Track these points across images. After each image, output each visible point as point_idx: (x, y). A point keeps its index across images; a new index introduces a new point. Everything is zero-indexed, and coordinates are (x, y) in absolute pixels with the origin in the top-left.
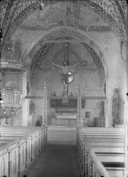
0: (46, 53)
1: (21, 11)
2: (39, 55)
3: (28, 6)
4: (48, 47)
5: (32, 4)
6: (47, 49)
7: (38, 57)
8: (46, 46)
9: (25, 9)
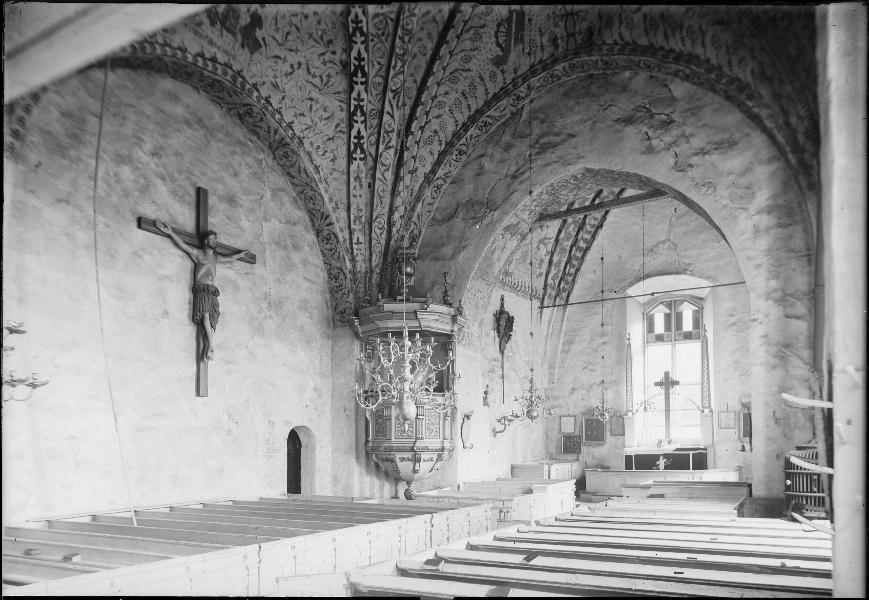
1: (443, 142)
2: (565, 259)
3: (460, 123)
4: (592, 226)
5: (472, 113)
9: (454, 135)
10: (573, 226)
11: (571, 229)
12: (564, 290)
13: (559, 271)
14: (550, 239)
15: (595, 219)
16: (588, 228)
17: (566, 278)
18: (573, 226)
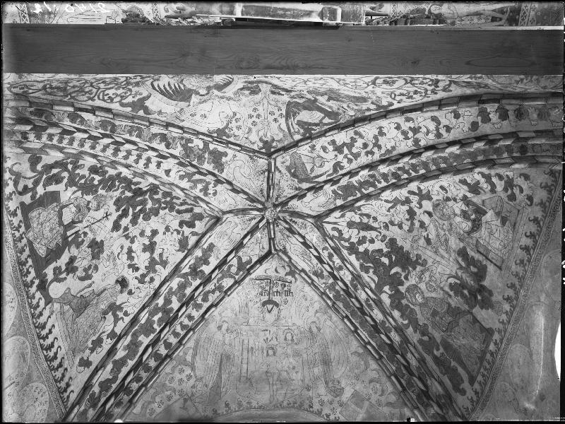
0: (167, 356)
2: (131, 363)
4: (183, 327)
6: (176, 334)
7: (125, 370)
8: (176, 317)
10: (160, 315)
11: (156, 318)
13: (115, 379)
14: (126, 314)
15: (190, 318)
17: (121, 395)
18: (160, 315)
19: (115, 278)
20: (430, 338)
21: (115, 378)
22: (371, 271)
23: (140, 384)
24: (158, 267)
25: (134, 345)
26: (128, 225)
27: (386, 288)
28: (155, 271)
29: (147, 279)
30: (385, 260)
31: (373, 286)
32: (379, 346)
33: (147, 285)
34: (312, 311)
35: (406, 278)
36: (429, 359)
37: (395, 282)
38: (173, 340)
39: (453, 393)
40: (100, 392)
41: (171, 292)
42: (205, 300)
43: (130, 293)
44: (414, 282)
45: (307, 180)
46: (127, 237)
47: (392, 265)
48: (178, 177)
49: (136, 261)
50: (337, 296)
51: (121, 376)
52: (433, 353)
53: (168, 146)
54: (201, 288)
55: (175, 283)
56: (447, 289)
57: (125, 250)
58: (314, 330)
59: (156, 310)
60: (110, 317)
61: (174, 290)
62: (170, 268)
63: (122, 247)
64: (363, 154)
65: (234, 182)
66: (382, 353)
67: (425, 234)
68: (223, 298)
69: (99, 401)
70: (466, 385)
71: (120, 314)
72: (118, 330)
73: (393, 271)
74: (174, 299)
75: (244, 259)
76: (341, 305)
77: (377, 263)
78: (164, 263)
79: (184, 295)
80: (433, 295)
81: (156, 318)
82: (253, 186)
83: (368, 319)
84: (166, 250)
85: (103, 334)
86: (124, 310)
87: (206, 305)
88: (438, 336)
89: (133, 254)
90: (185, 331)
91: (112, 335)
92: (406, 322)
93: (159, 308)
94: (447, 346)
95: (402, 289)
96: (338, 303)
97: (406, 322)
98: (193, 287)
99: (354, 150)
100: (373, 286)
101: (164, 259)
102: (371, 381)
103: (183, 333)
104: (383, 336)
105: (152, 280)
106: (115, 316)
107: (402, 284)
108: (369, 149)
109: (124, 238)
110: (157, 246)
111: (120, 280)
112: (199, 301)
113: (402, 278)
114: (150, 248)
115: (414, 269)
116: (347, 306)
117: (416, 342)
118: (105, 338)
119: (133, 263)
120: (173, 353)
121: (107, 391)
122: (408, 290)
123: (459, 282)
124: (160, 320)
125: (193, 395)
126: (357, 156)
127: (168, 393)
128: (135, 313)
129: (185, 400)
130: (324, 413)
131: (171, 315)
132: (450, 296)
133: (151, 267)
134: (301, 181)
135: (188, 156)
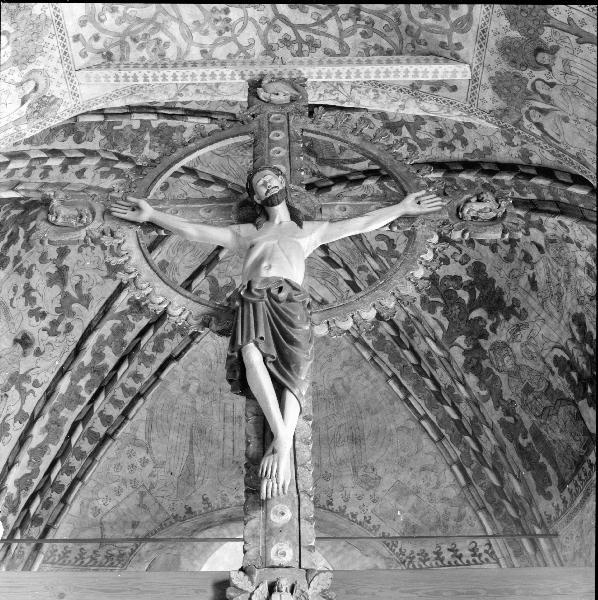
2: (54, 450)
4: (127, 392)
8: (113, 379)
10: (88, 377)
11: (82, 383)
12: (37, 520)
13: (36, 471)
14: (36, 384)
15: (136, 377)
16: (119, 394)
18: (88, 377)
19: (13, 338)
20: (516, 420)
21: (36, 471)
22: (439, 309)
23: (74, 476)
24: (75, 306)
25: (56, 423)
26: (19, 252)
27: (461, 340)
28: (72, 314)
29: (61, 328)
30: (464, 296)
31: (440, 333)
32: (440, 422)
33: (61, 338)
34: (337, 363)
35: (493, 329)
36: (510, 447)
37: (476, 333)
38: (115, 413)
39: (536, 495)
40: (19, 492)
41: (101, 342)
42: (158, 348)
43: (38, 353)
44: (503, 339)
45: (333, 162)
46: (19, 271)
47: (473, 306)
48: (98, 176)
49: (39, 303)
50: (381, 341)
51: (44, 467)
52: (517, 439)
53: (78, 140)
54: (151, 332)
55: (106, 329)
56: (550, 361)
57: (21, 291)
58: (340, 389)
59: (83, 371)
60: (14, 393)
61: (105, 338)
62: (96, 307)
63: (15, 290)
64: (435, 145)
65: (198, 168)
66: (443, 431)
67: (530, 272)
68: (189, 346)
69: (19, 502)
70: (553, 489)
71: (28, 386)
72: (29, 408)
73: (475, 314)
74: (108, 351)
75: (222, 282)
76: (385, 357)
77: (449, 298)
78: (86, 300)
79: (123, 343)
80: (530, 364)
81: (82, 383)
82: (235, 167)
83: (428, 382)
84: (85, 279)
85: (8, 418)
86: (32, 380)
87: (161, 358)
88: (527, 419)
89: (33, 294)
90: (130, 398)
91: (20, 416)
92: (484, 393)
93: (87, 368)
94: (538, 436)
95: (486, 344)
96: (380, 354)
97: (484, 393)
98: (136, 331)
99: (422, 136)
100: (440, 333)
101: (85, 292)
102: (423, 469)
103: (127, 401)
104: (449, 410)
105: (69, 328)
106: (21, 390)
107: (485, 336)
108: (446, 139)
109: (15, 276)
110: (70, 272)
111: (19, 338)
112: (149, 352)
113: (487, 328)
114: (60, 276)
115: (507, 319)
116: (395, 359)
117: (495, 422)
118: (10, 419)
119: (36, 307)
120: (116, 432)
121: (27, 489)
122: (495, 347)
123: (568, 358)
124: (89, 385)
125: (152, 486)
126: (424, 144)
127: (115, 485)
128: (51, 380)
129: (142, 495)
130: (348, 512)
131: (106, 375)
132: (553, 373)
133: (64, 309)
134: (322, 162)
135: (114, 145)
